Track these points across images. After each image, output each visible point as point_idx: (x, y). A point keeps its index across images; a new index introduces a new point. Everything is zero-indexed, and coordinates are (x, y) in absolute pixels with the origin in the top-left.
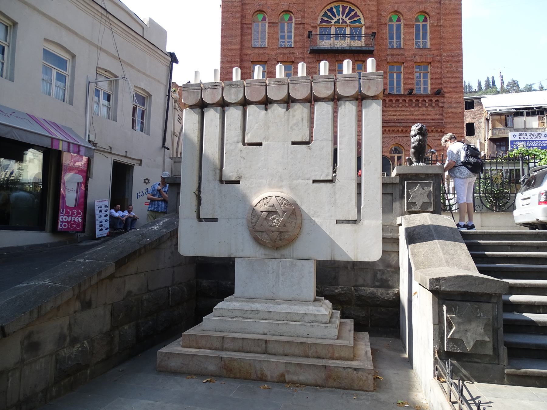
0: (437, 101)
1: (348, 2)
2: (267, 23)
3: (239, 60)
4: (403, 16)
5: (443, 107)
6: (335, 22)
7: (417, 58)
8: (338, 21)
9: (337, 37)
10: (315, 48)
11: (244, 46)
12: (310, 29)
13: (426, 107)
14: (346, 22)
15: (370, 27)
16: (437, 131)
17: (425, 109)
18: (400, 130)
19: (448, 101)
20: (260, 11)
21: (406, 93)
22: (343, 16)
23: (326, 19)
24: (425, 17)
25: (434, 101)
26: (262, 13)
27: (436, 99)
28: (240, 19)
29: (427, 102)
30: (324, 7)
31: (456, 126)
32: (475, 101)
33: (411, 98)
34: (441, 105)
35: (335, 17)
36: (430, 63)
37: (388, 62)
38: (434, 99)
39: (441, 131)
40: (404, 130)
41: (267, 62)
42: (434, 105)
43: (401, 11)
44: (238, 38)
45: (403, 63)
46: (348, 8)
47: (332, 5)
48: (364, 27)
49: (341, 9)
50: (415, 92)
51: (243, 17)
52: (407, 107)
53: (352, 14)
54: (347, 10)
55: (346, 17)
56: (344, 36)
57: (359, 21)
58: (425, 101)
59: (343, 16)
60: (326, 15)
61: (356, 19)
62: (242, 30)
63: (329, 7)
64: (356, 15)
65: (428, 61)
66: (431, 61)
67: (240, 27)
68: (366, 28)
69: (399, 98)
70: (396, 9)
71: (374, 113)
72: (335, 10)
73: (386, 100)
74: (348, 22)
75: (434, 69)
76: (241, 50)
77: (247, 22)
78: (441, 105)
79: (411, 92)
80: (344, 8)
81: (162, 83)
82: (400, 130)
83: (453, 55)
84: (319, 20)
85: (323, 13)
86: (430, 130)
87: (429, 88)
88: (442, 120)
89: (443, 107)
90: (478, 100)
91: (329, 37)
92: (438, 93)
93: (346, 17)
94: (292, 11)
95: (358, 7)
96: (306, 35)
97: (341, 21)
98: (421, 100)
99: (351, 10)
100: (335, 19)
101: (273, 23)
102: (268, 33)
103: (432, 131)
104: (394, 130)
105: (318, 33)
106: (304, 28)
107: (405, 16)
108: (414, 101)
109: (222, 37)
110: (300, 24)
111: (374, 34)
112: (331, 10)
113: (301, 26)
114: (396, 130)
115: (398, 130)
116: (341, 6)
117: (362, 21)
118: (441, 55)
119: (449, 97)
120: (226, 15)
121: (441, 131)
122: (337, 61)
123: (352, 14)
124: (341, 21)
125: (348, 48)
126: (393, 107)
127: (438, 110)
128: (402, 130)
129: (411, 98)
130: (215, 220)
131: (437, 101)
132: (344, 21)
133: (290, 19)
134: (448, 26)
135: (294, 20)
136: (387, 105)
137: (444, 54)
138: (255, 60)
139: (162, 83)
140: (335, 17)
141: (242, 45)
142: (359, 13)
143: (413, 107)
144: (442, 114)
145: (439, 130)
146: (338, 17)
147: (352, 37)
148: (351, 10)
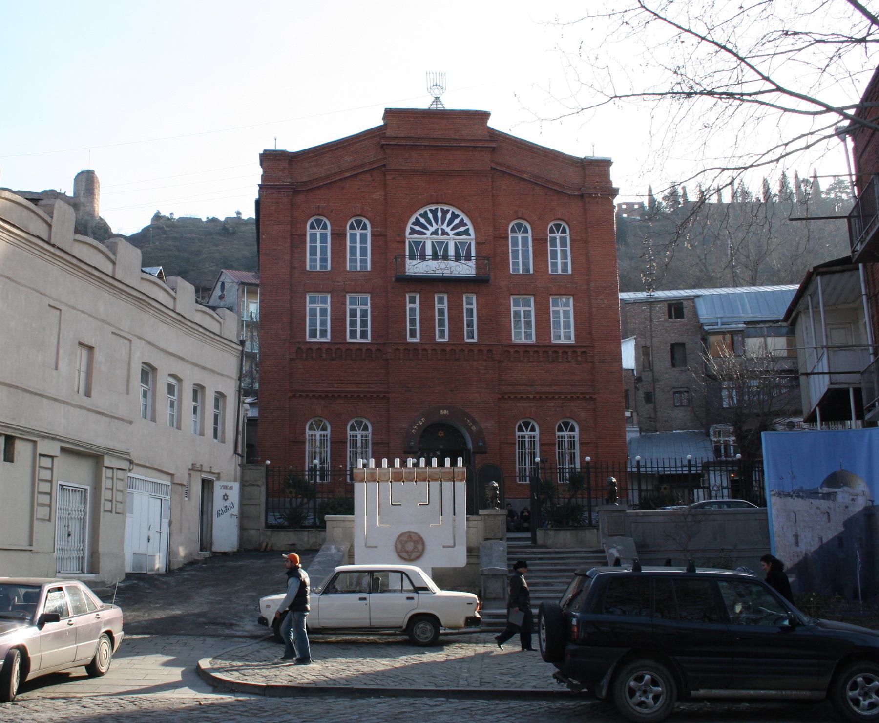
5: (592, 362)
6: (432, 234)
8: (435, 233)
11: (295, 268)
13: (569, 362)
14: (448, 234)
22: (443, 223)
23: (417, 228)
25: (579, 354)
28: (289, 228)
29: (570, 354)
32: (685, 303)
35: (432, 225)
53: (457, 221)
54: (449, 216)
58: (567, 353)
61: (462, 229)
67: (289, 241)
69: (528, 349)
74: (451, 233)
81: (231, 378)
90: (690, 303)
97: (440, 232)
100: (432, 229)
114: (525, 396)
115: (528, 397)
123: (457, 221)
124: (440, 232)
132: (444, 233)
137: (592, 284)
139: (231, 378)
140: (432, 225)
141: (293, 268)
145: (588, 396)
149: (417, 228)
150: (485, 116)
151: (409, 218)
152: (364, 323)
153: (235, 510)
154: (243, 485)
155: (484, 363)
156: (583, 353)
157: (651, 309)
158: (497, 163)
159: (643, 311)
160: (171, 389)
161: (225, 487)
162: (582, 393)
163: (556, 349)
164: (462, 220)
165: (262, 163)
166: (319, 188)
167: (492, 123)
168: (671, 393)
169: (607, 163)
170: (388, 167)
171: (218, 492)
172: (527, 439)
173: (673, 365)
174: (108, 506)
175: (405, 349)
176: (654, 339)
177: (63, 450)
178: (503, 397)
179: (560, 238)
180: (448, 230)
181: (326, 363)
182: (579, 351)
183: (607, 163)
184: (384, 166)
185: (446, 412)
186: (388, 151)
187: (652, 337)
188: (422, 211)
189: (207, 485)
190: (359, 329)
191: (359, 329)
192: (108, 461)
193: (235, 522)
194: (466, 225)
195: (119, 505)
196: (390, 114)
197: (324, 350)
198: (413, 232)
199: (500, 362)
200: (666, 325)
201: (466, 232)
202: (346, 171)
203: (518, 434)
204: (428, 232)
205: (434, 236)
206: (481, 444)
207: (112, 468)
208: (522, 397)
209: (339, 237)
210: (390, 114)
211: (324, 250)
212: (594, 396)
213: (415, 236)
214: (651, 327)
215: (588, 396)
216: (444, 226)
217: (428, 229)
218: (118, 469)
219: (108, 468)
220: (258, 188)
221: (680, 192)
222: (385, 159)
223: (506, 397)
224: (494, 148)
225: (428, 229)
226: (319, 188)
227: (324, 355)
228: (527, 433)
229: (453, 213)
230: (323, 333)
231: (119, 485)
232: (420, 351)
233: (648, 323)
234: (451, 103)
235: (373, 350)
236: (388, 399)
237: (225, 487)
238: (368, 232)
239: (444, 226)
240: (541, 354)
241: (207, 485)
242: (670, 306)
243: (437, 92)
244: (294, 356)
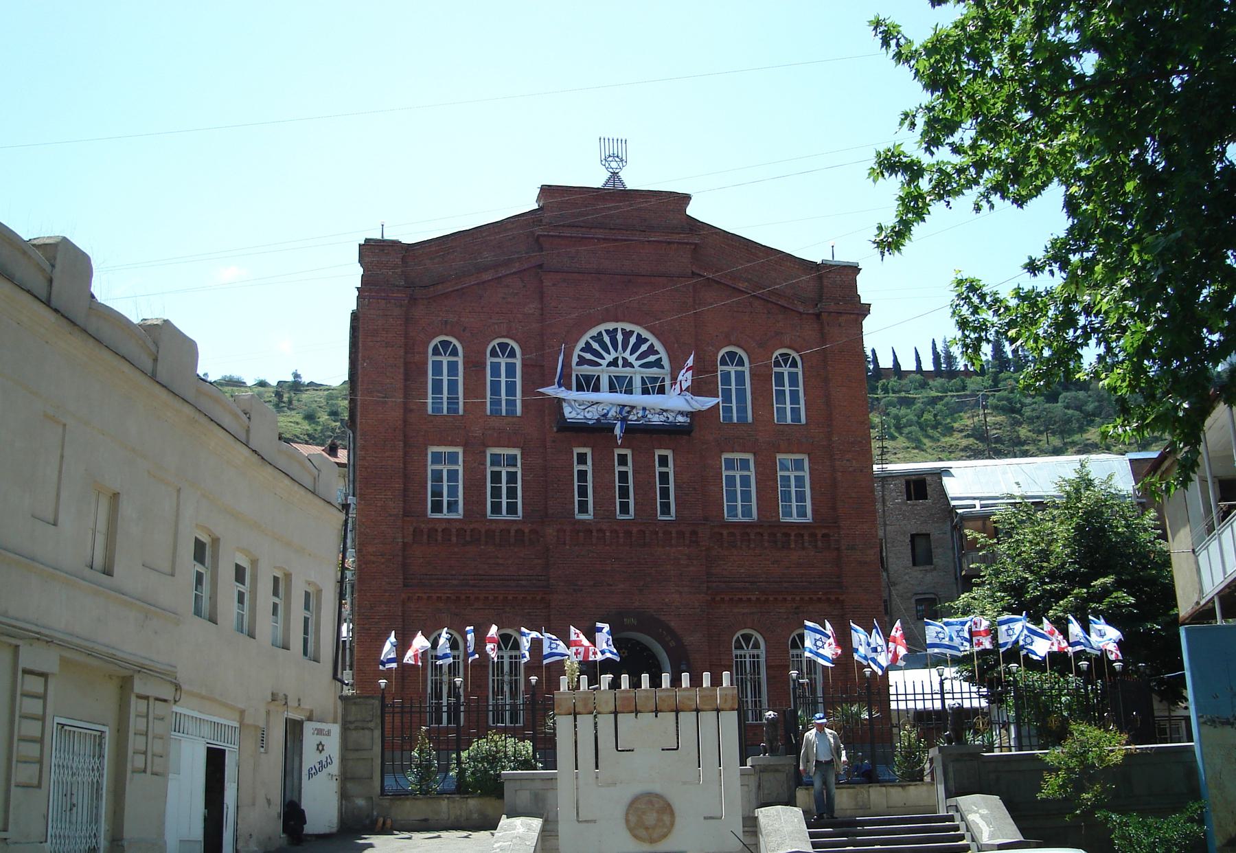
6: (609, 365)
8: (614, 363)
11: (411, 411)
13: (803, 548)
14: (631, 366)
16: (828, 599)
18: (753, 598)
22: (624, 350)
23: (588, 356)
25: (819, 536)
28: (402, 352)
29: (806, 538)
32: (928, 479)
40: (763, 599)
42: (819, 543)
58: (802, 536)
61: (652, 358)
62: (407, 378)
67: (402, 370)
69: (748, 530)
71: (730, 720)
74: (637, 364)
76: (405, 421)
82: (753, 598)
89: (838, 549)
97: (620, 362)
100: (609, 358)
104: (741, 599)
114: (744, 598)
115: (749, 600)
123: (644, 347)
124: (620, 362)
128: (758, 599)
130: (595, 821)
132: (627, 364)
137: (835, 438)
141: (407, 410)
145: (833, 598)
149: (588, 356)
151: (577, 341)
152: (512, 493)
153: (335, 768)
154: (345, 729)
156: (824, 536)
157: (883, 487)
160: (240, 574)
161: (320, 732)
164: (652, 346)
165: (361, 260)
166: (446, 295)
167: (692, 210)
168: (913, 601)
171: (310, 739)
172: (748, 659)
173: (914, 564)
174: (139, 762)
176: (888, 528)
177: (64, 662)
179: (789, 373)
180: (632, 359)
182: (820, 533)
184: (541, 266)
185: (633, 621)
187: (885, 525)
188: (594, 332)
189: (294, 730)
190: (504, 501)
191: (504, 501)
192: (139, 687)
193: (334, 786)
195: (157, 760)
198: (582, 360)
200: (904, 508)
201: (658, 364)
203: (735, 652)
204: (604, 363)
207: (147, 698)
209: (475, 366)
211: (453, 385)
215: (833, 598)
216: (627, 355)
217: (603, 358)
218: (157, 699)
219: (139, 697)
221: (869, 353)
223: (718, 598)
225: (603, 358)
226: (446, 295)
227: (454, 539)
228: (748, 652)
230: (452, 506)
231: (157, 728)
232: (595, 534)
234: (635, 179)
235: (527, 531)
237: (320, 732)
238: (518, 362)
239: (627, 355)
241: (294, 730)
242: (908, 483)
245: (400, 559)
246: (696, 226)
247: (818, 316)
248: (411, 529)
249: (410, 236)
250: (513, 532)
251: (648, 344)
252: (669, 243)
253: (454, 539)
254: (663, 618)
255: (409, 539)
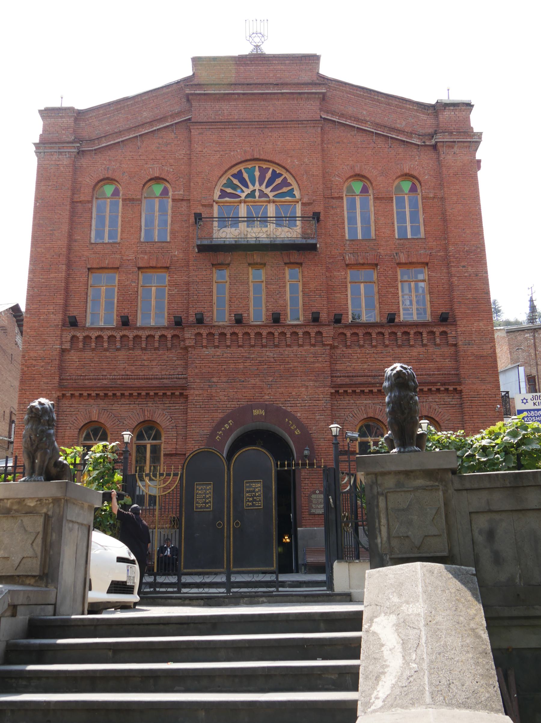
0: (444, 333)
1: (268, 161)
2: (121, 200)
3: (64, 267)
4: (371, 183)
5: (455, 345)
6: (248, 196)
7: (402, 255)
8: (252, 195)
9: (250, 220)
10: (206, 242)
12: (199, 209)
13: (424, 345)
14: (266, 196)
15: (309, 204)
16: (447, 390)
17: (422, 349)
19: (463, 333)
20: (108, 179)
21: (385, 321)
22: (261, 184)
23: (229, 190)
24: (414, 185)
25: (437, 334)
26: (112, 184)
27: (442, 329)
28: (69, 194)
29: (425, 335)
30: (226, 172)
31: (483, 381)
33: (394, 330)
34: (451, 341)
35: (247, 187)
36: (427, 264)
37: (347, 265)
38: (438, 330)
39: (455, 389)
41: (118, 268)
42: (438, 341)
43: (368, 176)
44: (65, 228)
45: (376, 265)
46: (270, 171)
47: (241, 167)
48: (300, 203)
49: (257, 174)
50: (402, 317)
51: (74, 190)
52: (387, 346)
53: (279, 181)
55: (267, 187)
56: (264, 220)
57: (291, 193)
58: (421, 334)
59: (261, 184)
60: (229, 184)
61: (285, 190)
62: (73, 213)
63: (235, 170)
64: (285, 183)
65: (423, 260)
66: (427, 261)
67: (68, 207)
68: (303, 204)
69: (369, 330)
70: (357, 171)
72: (246, 176)
73: (345, 335)
74: (271, 195)
75: (434, 274)
76: (69, 249)
77: (82, 198)
78: (451, 341)
79: (392, 319)
80: (263, 172)
83: (467, 248)
84: (217, 193)
85: (223, 181)
86: (434, 389)
87: (429, 311)
88: (457, 369)
89: (455, 345)
91: (235, 220)
92: (444, 319)
93: (267, 187)
94: (168, 178)
95: (287, 170)
96: (192, 220)
98: (412, 332)
99: (276, 175)
100: (247, 191)
101: (133, 200)
102: (122, 217)
103: (438, 390)
105: (216, 215)
106: (189, 207)
107: (374, 183)
108: (399, 334)
109: (34, 225)
110: (182, 200)
111: (316, 217)
112: (239, 176)
113: (184, 203)
114: (366, 390)
115: (371, 392)
116: (257, 168)
117: (297, 193)
118: (446, 249)
119: (464, 325)
120: (44, 188)
121: (455, 389)
122: (249, 264)
124: (257, 194)
125: (266, 241)
126: (361, 347)
127: (448, 351)
129: (394, 330)
131: (444, 333)
132: (263, 194)
133: (165, 192)
134: (455, 198)
135: (170, 194)
136: (349, 344)
137: (451, 248)
138: (95, 266)
140: (247, 187)
142: (290, 180)
143: (399, 346)
144: (456, 357)
145: (451, 388)
146: (251, 188)
147: (279, 220)
148: (276, 175)
150: (312, 60)
155: (313, 349)
157: (534, 336)
158: (327, 112)
159: (526, 339)
162: (443, 384)
163: (406, 329)
169: (469, 106)
170: (193, 120)
175: (211, 334)
178: (337, 392)
180: (267, 191)
181: (108, 354)
183: (469, 106)
184: (189, 119)
185: (263, 413)
186: (195, 104)
187: (537, 364)
194: (290, 185)
196: (196, 61)
197: (106, 338)
199: (333, 347)
202: (143, 125)
205: (249, 199)
206: (306, 452)
208: (362, 392)
210: (196, 61)
212: (459, 388)
213: (227, 199)
214: (536, 355)
215: (451, 388)
220: (34, 148)
222: (190, 111)
223: (341, 391)
224: (324, 94)
229: (274, 171)
232: (228, 336)
233: (532, 351)
235: (169, 336)
236: (186, 397)
240: (387, 336)
243: (257, 40)
244: (67, 346)
245: (57, 362)
246: (325, 81)
247: (435, 147)
248: (69, 338)
249: (82, 105)
250: (157, 338)
251: (283, 177)
252: (300, 93)
253: (106, 345)
254: (289, 409)
255: (67, 346)
